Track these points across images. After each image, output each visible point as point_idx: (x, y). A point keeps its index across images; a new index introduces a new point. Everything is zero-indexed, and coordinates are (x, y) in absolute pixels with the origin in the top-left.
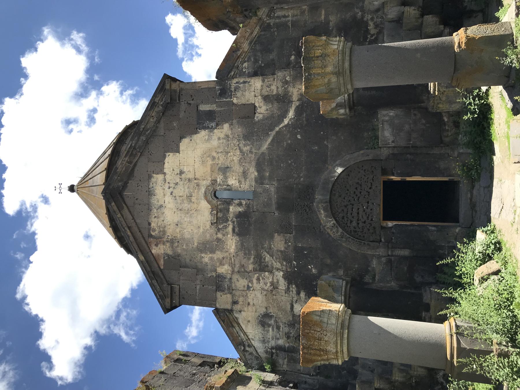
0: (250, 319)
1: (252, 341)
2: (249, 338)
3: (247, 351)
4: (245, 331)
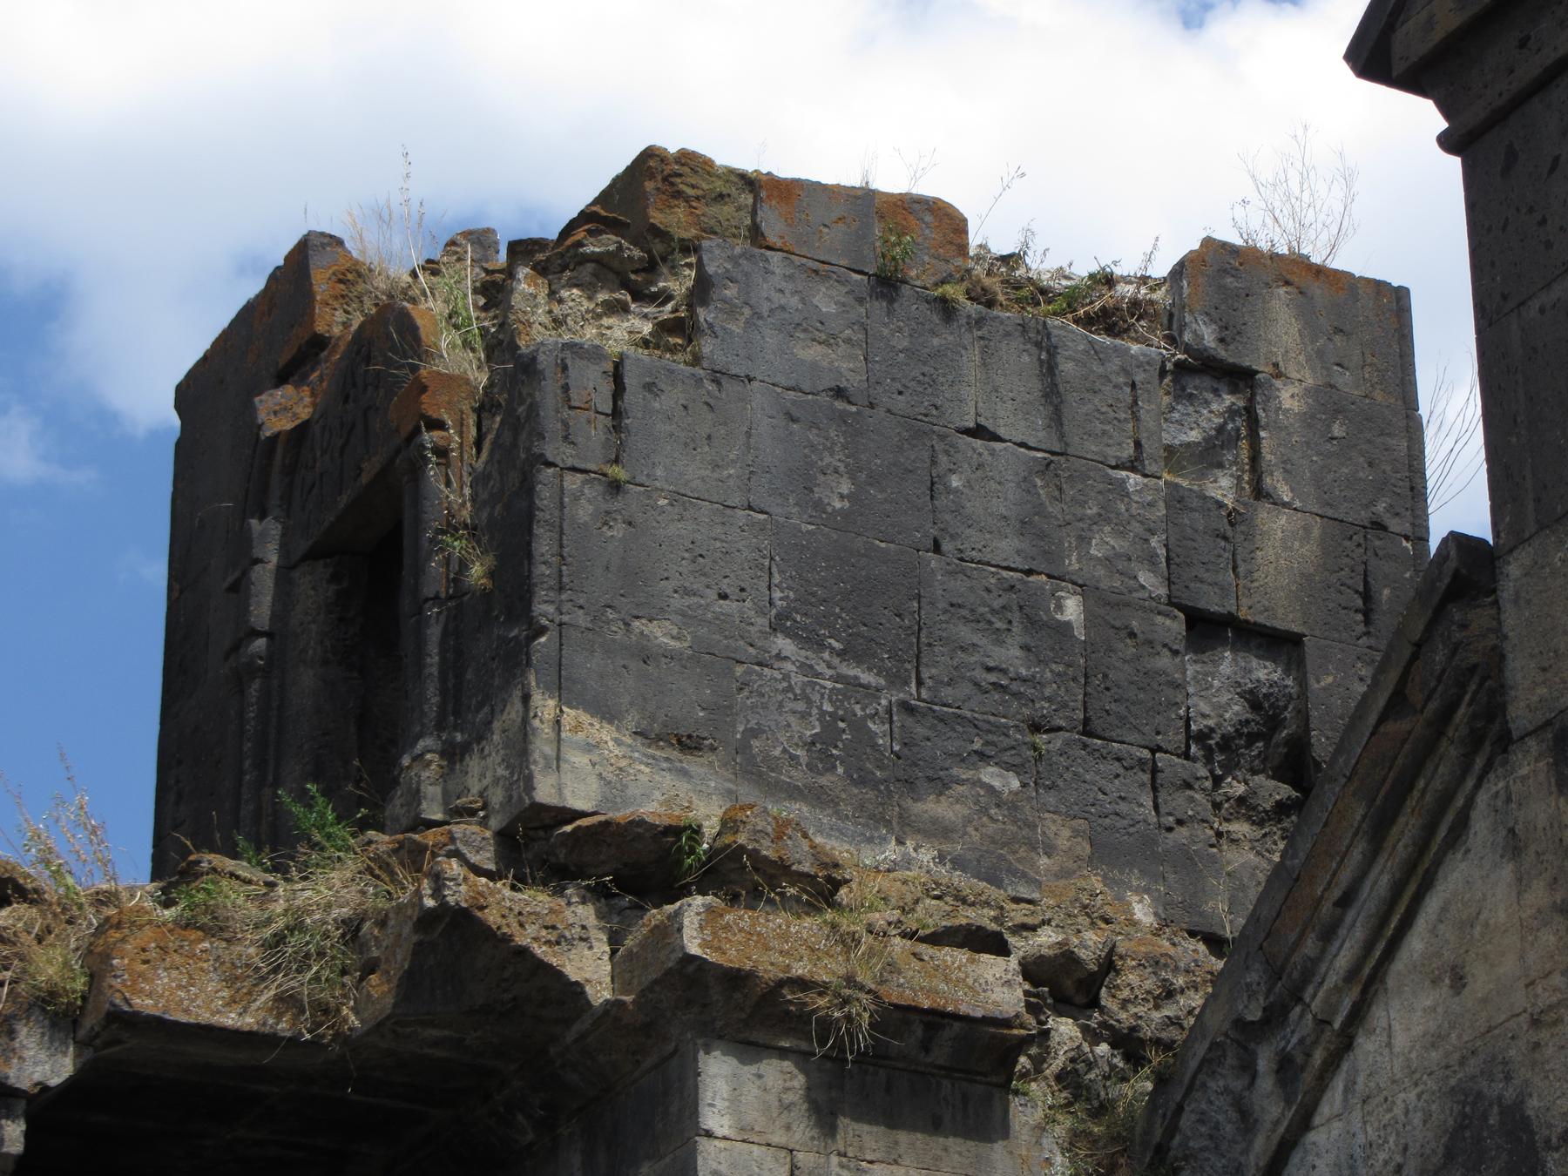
0: (1480, 981)
1: (1338, 1084)
2: (1345, 1043)
3: (1248, 1068)
4: (1391, 982)
